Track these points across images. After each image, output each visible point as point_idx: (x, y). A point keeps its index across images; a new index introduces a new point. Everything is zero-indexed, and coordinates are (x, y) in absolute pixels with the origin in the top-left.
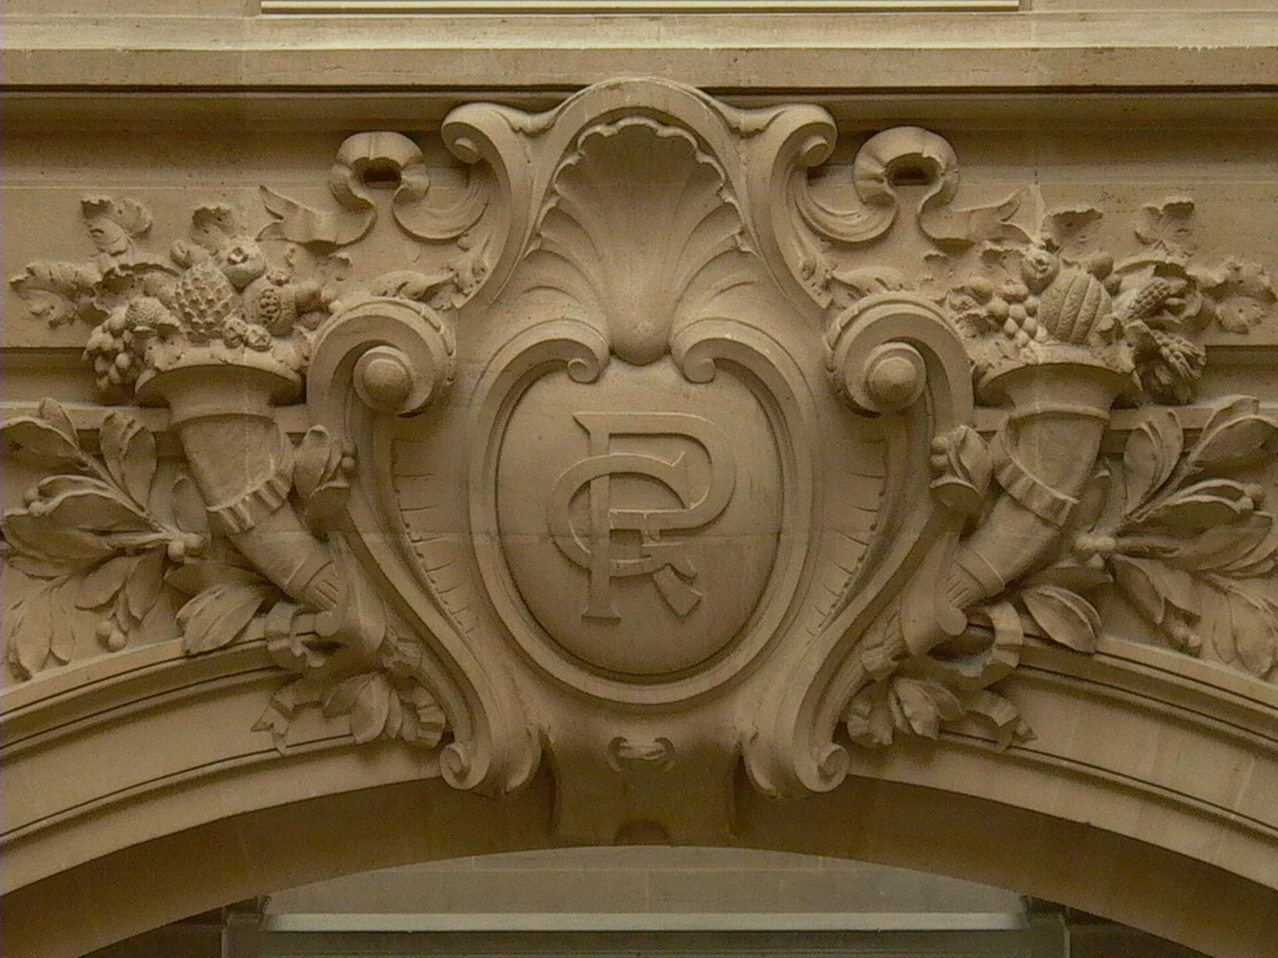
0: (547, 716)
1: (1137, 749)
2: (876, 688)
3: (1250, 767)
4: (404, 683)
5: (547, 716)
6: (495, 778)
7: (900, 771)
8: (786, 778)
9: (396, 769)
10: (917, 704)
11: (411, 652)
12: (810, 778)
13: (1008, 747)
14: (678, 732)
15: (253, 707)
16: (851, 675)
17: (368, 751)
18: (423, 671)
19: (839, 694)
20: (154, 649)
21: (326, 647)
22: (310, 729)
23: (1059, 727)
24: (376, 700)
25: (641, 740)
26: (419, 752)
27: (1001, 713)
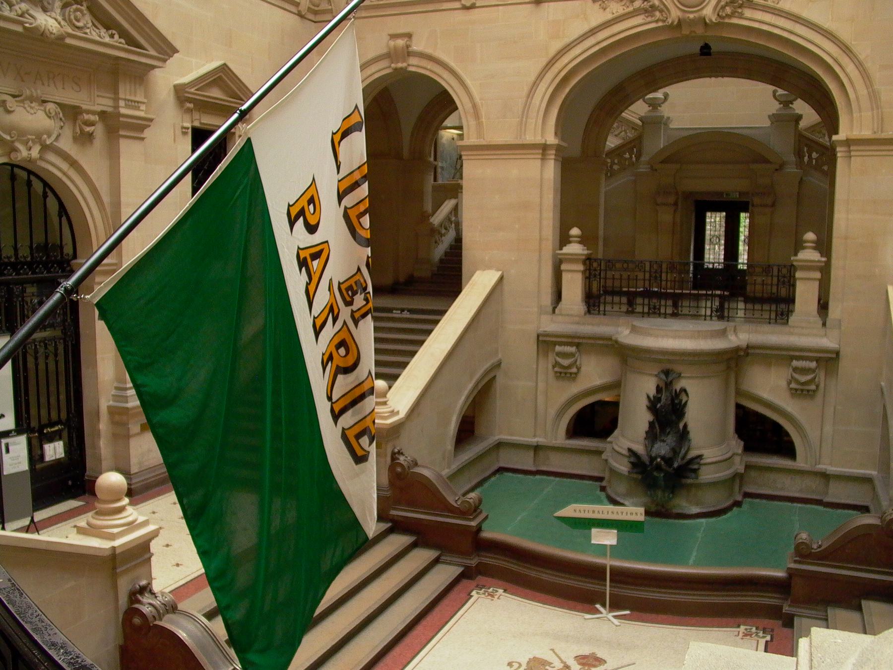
0: (679, 13)
1: (759, 15)
2: (723, 8)
3: (774, 17)
4: (661, 11)
5: (679, 13)
6: (672, 23)
7: (727, 21)
8: (711, 20)
9: (660, 24)
10: (728, 10)
11: (662, 6)
12: (714, 20)
13: (741, 16)
14: (696, 15)
15: (643, 16)
16: (720, 6)
17: (657, 21)
18: (664, 9)
19: (718, 9)
20: (631, 9)
21: (651, 7)
22: (649, 19)
23: (748, 13)
24: (658, 14)
25: (692, 16)
26: (664, 21)
27: (740, 10)
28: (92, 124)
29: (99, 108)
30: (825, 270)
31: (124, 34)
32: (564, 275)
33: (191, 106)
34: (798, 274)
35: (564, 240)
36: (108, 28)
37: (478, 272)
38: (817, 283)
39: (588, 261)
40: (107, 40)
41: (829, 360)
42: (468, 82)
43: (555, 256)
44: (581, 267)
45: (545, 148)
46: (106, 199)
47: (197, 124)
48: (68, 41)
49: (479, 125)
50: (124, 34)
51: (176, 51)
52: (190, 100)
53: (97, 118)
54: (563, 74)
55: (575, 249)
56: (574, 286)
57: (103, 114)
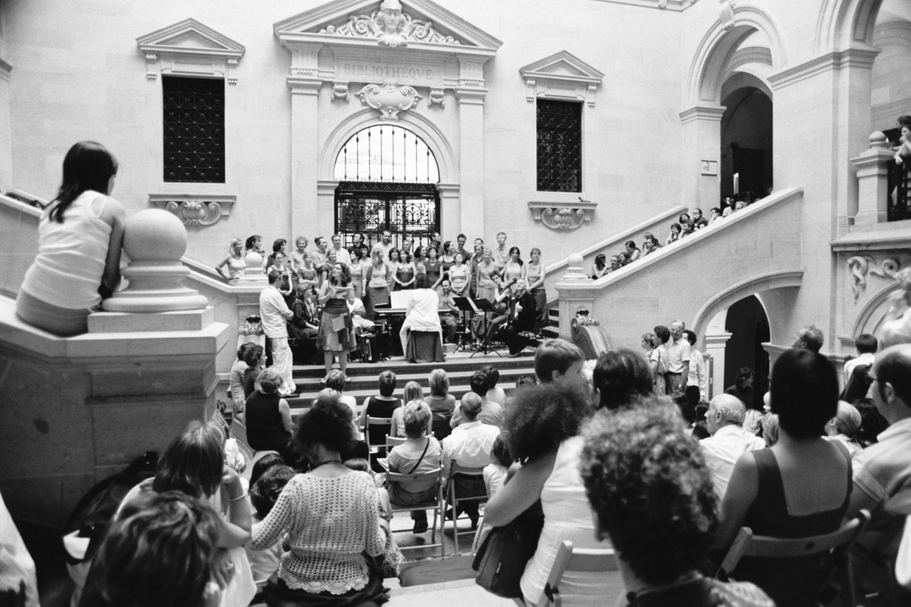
28: (440, 97)
29: (444, 87)
31: (456, 37)
33: (534, 82)
36: (445, 35)
40: (444, 43)
43: (851, 162)
46: (453, 144)
47: (542, 96)
48: (409, 46)
50: (456, 37)
51: (501, 43)
52: (531, 78)
53: (442, 93)
56: (872, 191)
57: (448, 91)
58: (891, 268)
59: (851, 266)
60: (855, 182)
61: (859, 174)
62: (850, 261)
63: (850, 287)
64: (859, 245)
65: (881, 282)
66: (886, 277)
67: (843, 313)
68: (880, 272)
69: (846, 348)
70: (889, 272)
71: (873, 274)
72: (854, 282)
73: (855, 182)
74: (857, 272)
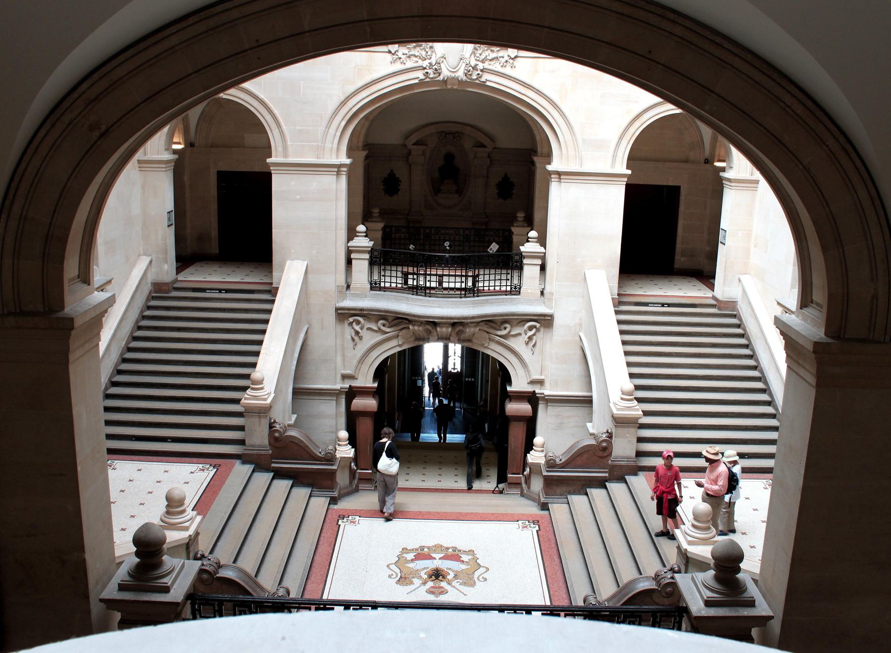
30: (543, 258)
32: (353, 261)
34: (525, 261)
35: (351, 234)
37: (288, 263)
38: (539, 268)
39: (372, 252)
41: (545, 321)
42: (276, 112)
44: (367, 256)
45: (340, 166)
49: (285, 148)
54: (355, 110)
55: (363, 242)
58: (384, 325)
59: (351, 324)
60: (349, 262)
61: (353, 256)
62: (351, 319)
63: (349, 337)
64: (362, 310)
65: (375, 334)
66: (380, 331)
67: (343, 356)
68: (375, 328)
69: (346, 380)
70: (383, 328)
71: (369, 329)
72: (353, 334)
73: (349, 262)
74: (357, 328)
